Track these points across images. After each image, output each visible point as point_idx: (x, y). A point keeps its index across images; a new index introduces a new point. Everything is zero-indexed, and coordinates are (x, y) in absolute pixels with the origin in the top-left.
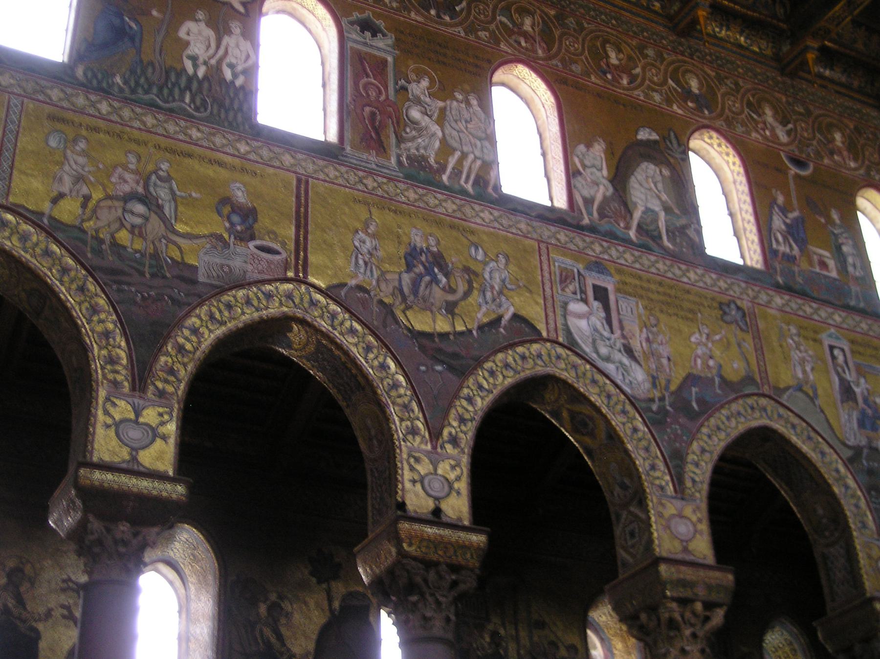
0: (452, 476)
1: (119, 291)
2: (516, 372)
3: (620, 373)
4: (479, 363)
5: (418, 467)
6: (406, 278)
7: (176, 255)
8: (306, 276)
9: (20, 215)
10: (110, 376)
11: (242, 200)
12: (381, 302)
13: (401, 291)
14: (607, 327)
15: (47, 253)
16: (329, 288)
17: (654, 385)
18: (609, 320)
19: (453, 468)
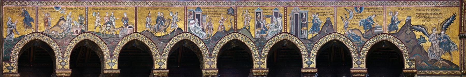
0: (163, 62)
1: (107, 42)
2: (178, 40)
3: (200, 35)
4: (170, 40)
5: (157, 61)
6: (156, 25)
7: (115, 33)
8: (137, 31)
9: (90, 33)
10: (107, 56)
11: (126, 17)
12: (151, 33)
13: (155, 29)
14: (198, 25)
15: (95, 38)
16: (141, 33)
17: (208, 36)
18: (199, 23)
19: (164, 60)
